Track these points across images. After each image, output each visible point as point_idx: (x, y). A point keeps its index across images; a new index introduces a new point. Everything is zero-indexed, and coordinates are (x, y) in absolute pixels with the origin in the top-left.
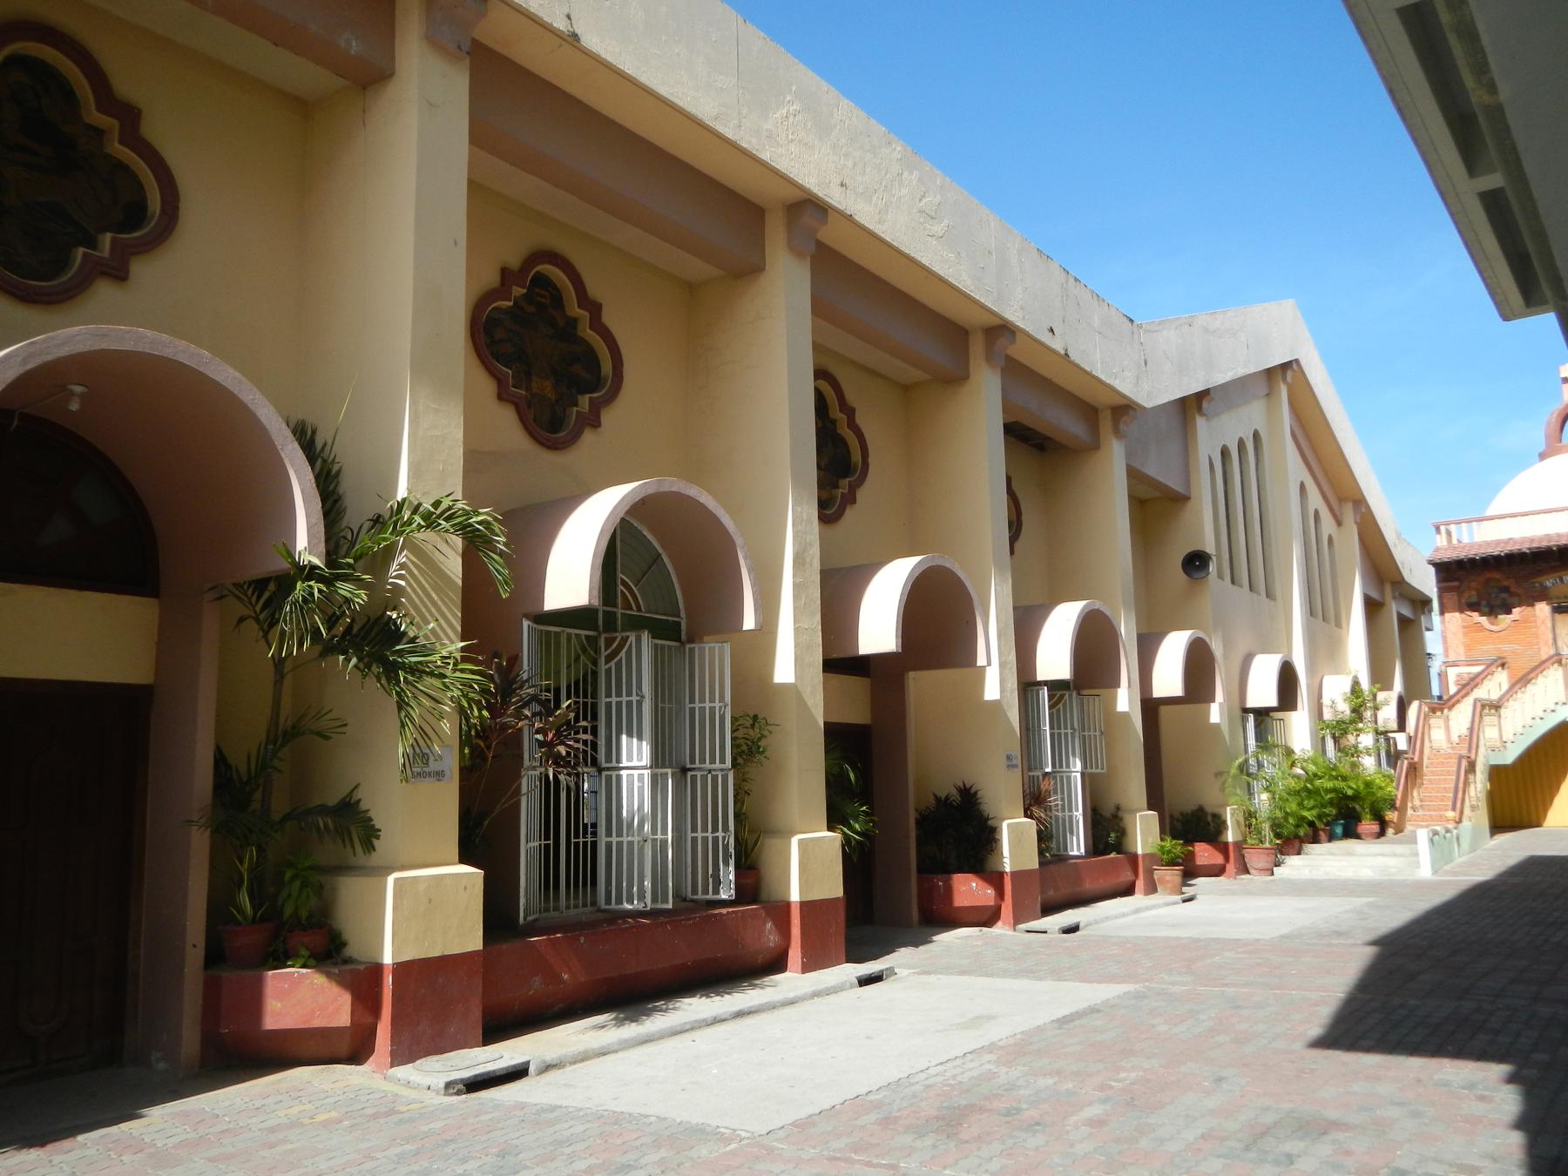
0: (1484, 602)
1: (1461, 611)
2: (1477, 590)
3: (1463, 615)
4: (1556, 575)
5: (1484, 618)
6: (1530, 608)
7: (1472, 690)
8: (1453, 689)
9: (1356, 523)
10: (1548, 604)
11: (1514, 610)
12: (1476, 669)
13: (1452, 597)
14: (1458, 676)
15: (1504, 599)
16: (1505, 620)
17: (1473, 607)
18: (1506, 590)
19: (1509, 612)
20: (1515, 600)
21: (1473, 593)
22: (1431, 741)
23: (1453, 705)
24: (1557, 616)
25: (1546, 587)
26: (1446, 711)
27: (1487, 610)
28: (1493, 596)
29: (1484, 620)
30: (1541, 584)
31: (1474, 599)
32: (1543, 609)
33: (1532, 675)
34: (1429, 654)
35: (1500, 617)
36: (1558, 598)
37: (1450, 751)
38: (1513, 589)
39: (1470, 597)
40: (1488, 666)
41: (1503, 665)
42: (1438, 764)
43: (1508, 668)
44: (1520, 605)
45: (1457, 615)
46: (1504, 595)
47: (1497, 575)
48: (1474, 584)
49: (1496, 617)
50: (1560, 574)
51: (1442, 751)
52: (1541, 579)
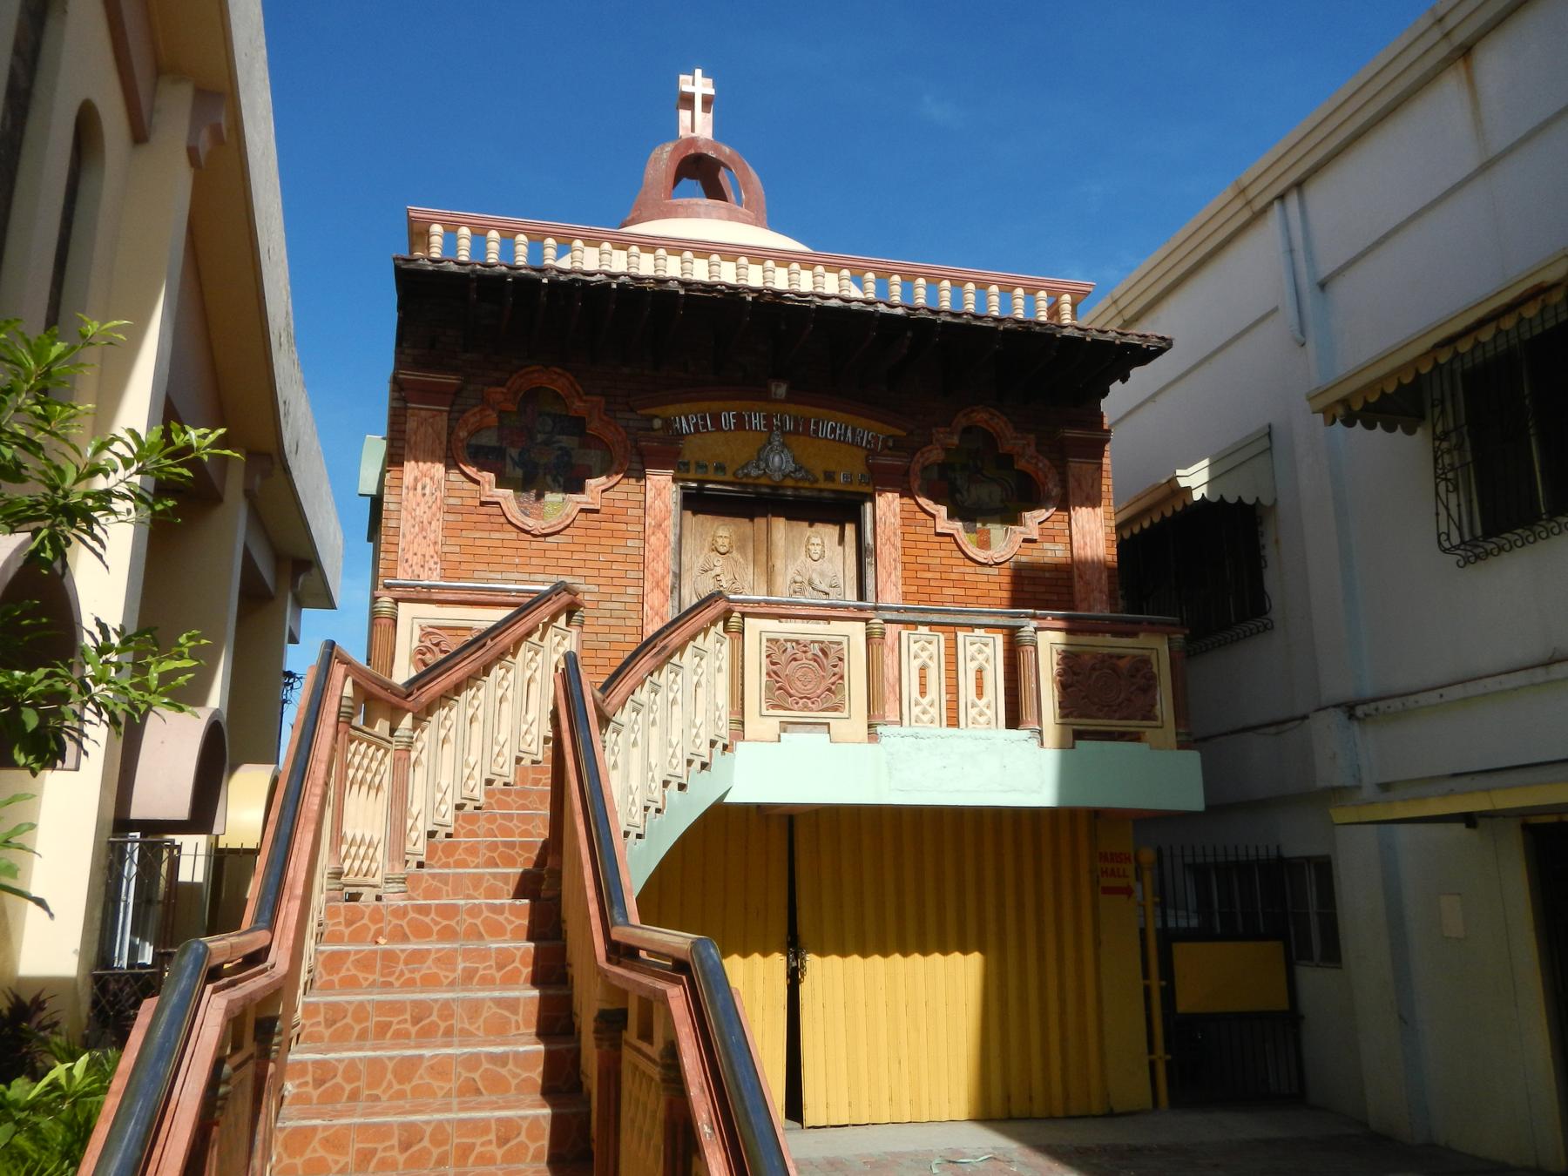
0: (514, 452)
1: (451, 463)
2: (502, 414)
3: (455, 476)
4: (705, 405)
5: (510, 492)
6: (632, 481)
7: (486, 670)
8: (403, 672)
9: (192, 153)
10: (675, 480)
11: (591, 483)
12: (501, 614)
13: (428, 419)
14: (426, 634)
15: (566, 452)
16: (558, 506)
17: (483, 457)
18: (577, 425)
19: (575, 485)
20: (594, 457)
21: (492, 417)
22: (338, 837)
23: (429, 710)
24: (688, 514)
25: (680, 435)
26: (407, 721)
27: (519, 473)
28: (540, 438)
29: (506, 495)
30: (668, 423)
31: (489, 439)
32: (662, 488)
33: (675, 639)
34: (290, 675)
35: (550, 497)
36: (701, 466)
37: (394, 899)
38: (594, 426)
39: (477, 431)
40: (523, 610)
41: (571, 610)
42: (365, 963)
43: (582, 624)
44: (606, 471)
45: (439, 469)
46: (566, 441)
47: (558, 381)
48: (497, 394)
49: (540, 496)
50: (715, 406)
51: (368, 896)
52: (671, 410)
